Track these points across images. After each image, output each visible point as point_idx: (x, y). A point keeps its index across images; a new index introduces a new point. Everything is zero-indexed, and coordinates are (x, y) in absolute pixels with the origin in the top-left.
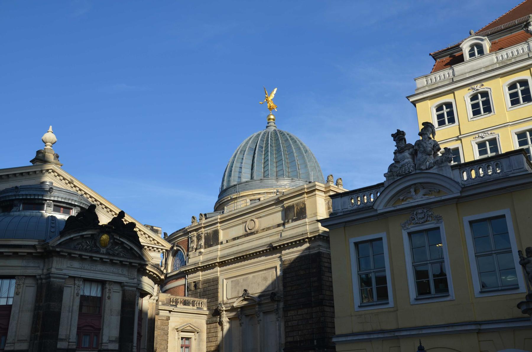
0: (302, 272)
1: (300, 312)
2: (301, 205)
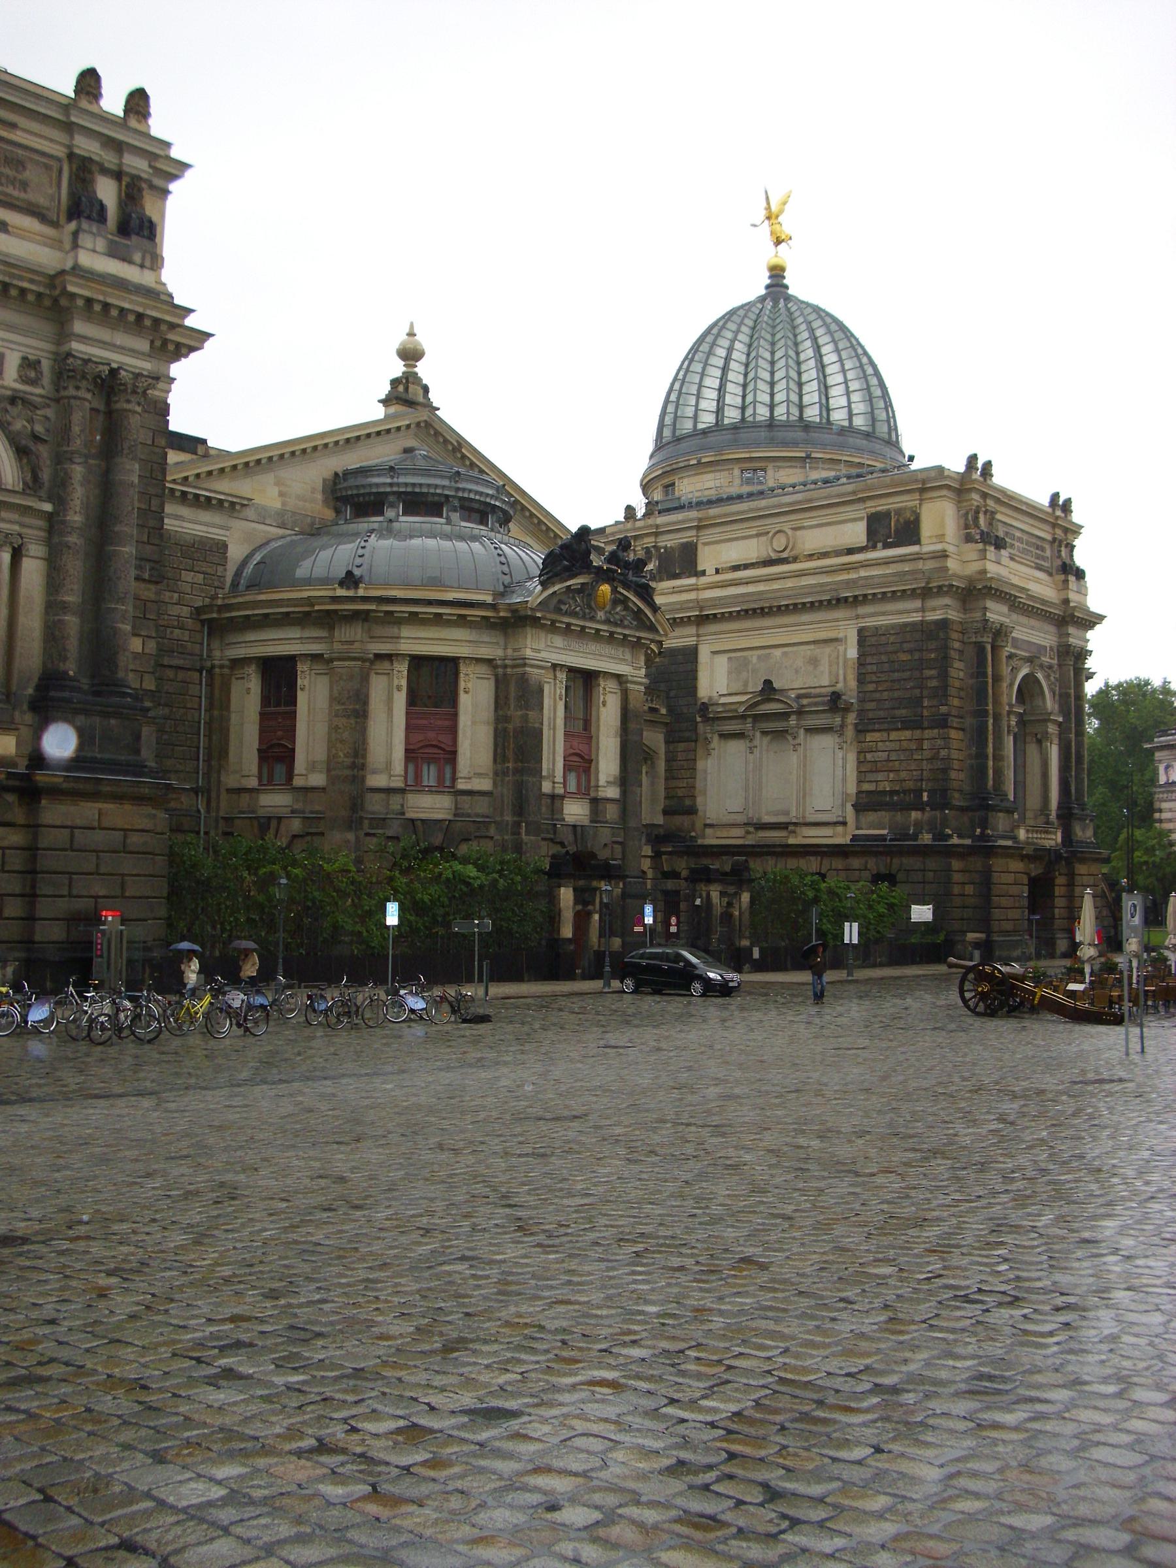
0: (904, 657)
1: (894, 735)
2: (908, 514)
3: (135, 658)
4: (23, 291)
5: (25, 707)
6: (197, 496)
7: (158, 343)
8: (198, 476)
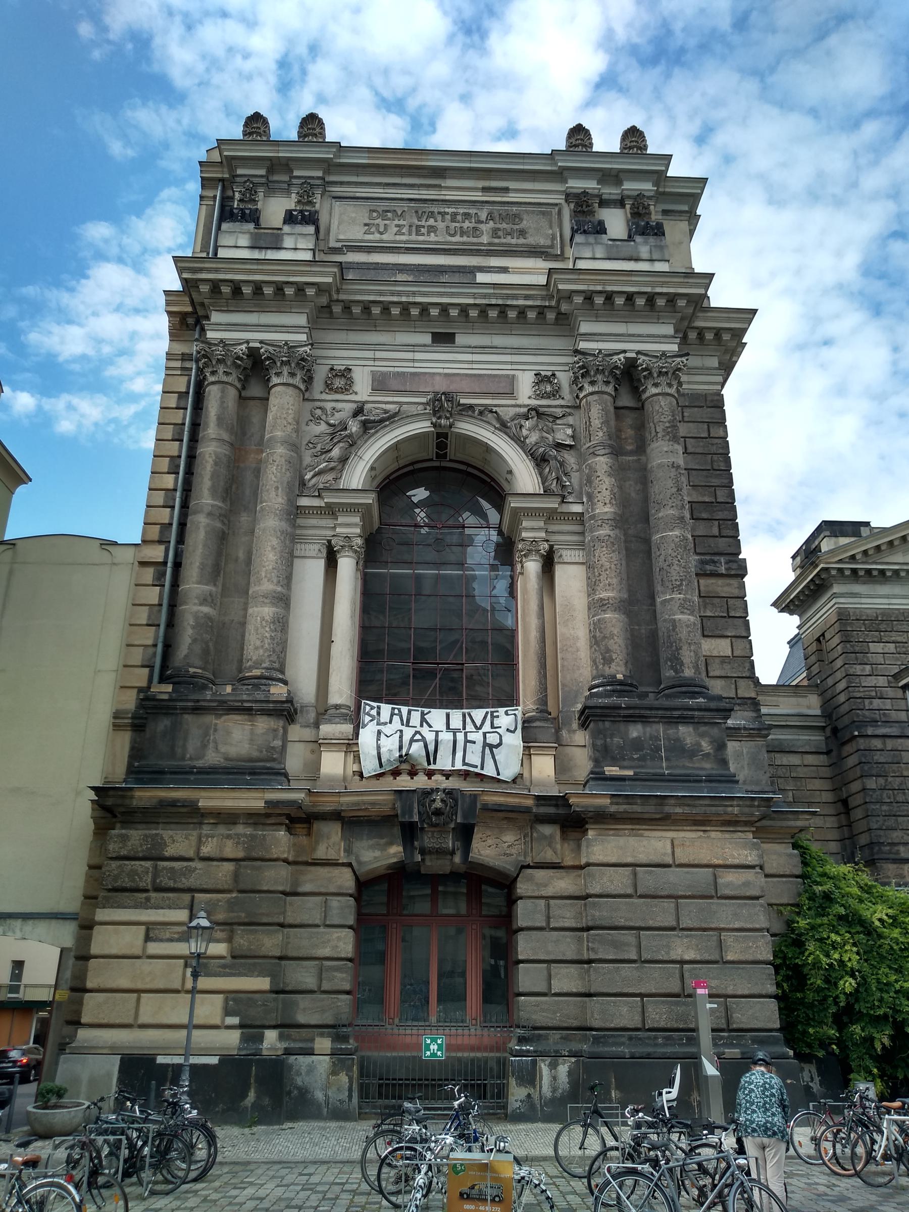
3: (723, 662)
4: (522, 312)
5: (575, 725)
6: (869, 572)
7: (693, 335)
8: (865, 552)
